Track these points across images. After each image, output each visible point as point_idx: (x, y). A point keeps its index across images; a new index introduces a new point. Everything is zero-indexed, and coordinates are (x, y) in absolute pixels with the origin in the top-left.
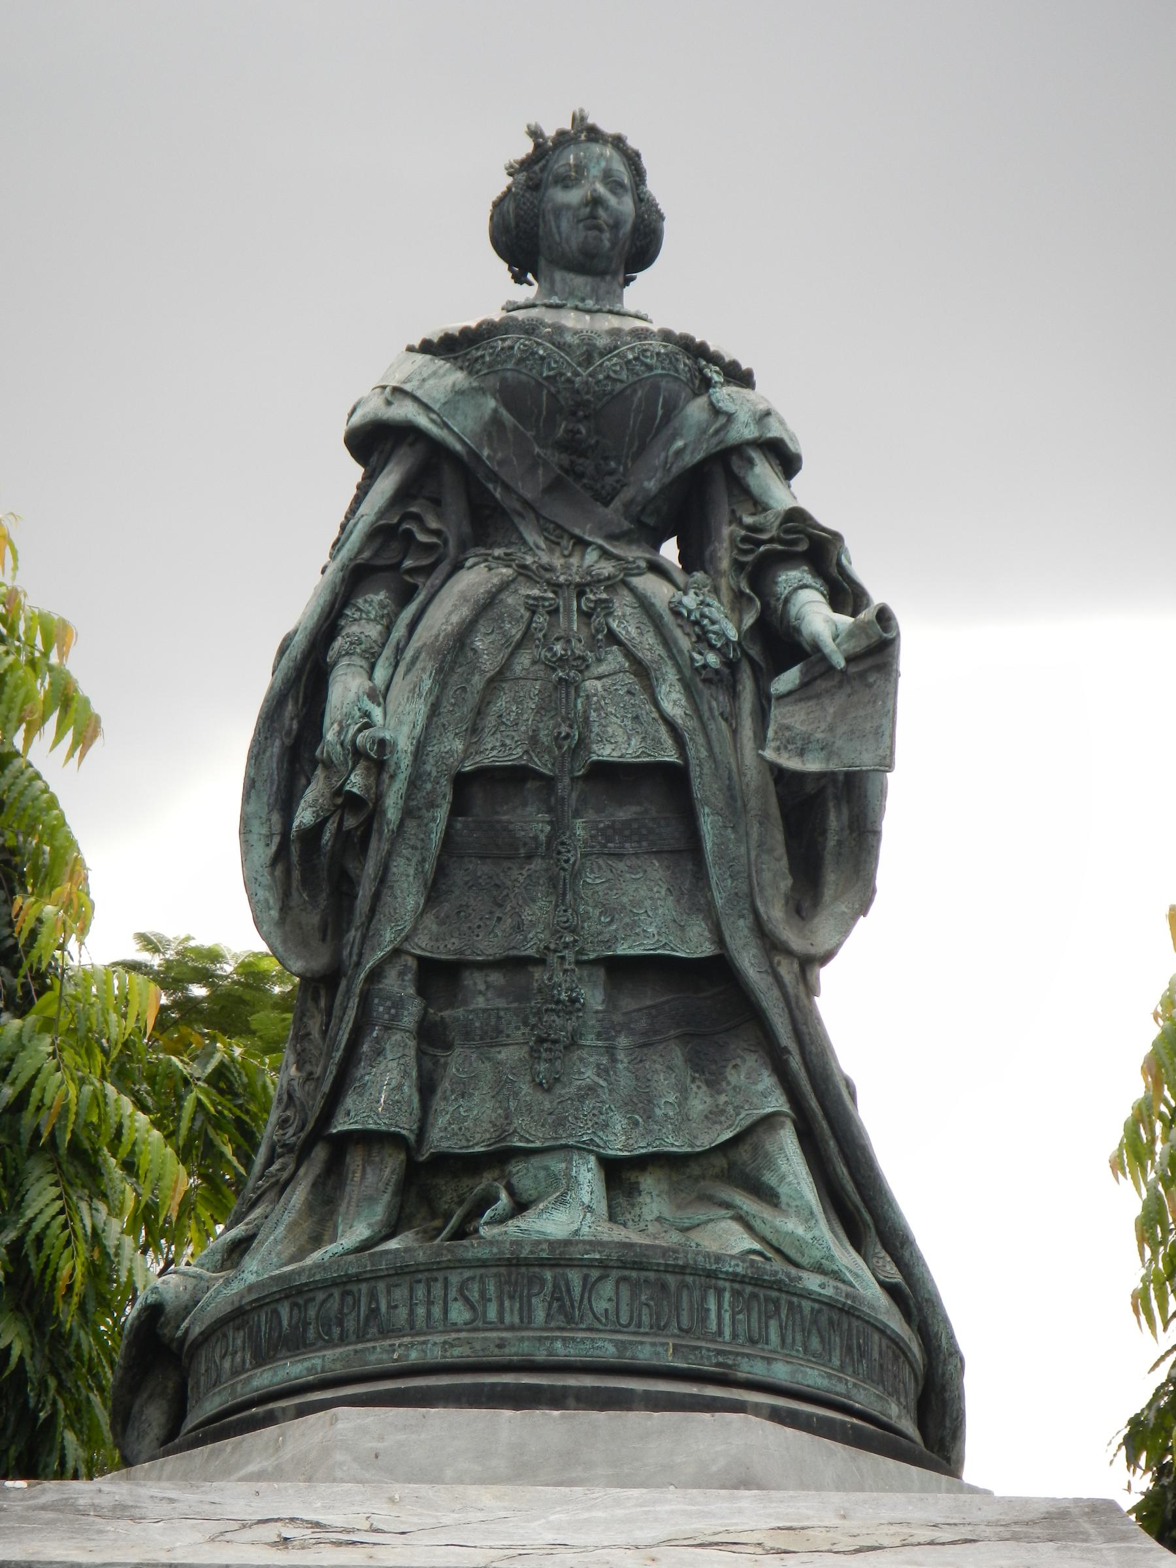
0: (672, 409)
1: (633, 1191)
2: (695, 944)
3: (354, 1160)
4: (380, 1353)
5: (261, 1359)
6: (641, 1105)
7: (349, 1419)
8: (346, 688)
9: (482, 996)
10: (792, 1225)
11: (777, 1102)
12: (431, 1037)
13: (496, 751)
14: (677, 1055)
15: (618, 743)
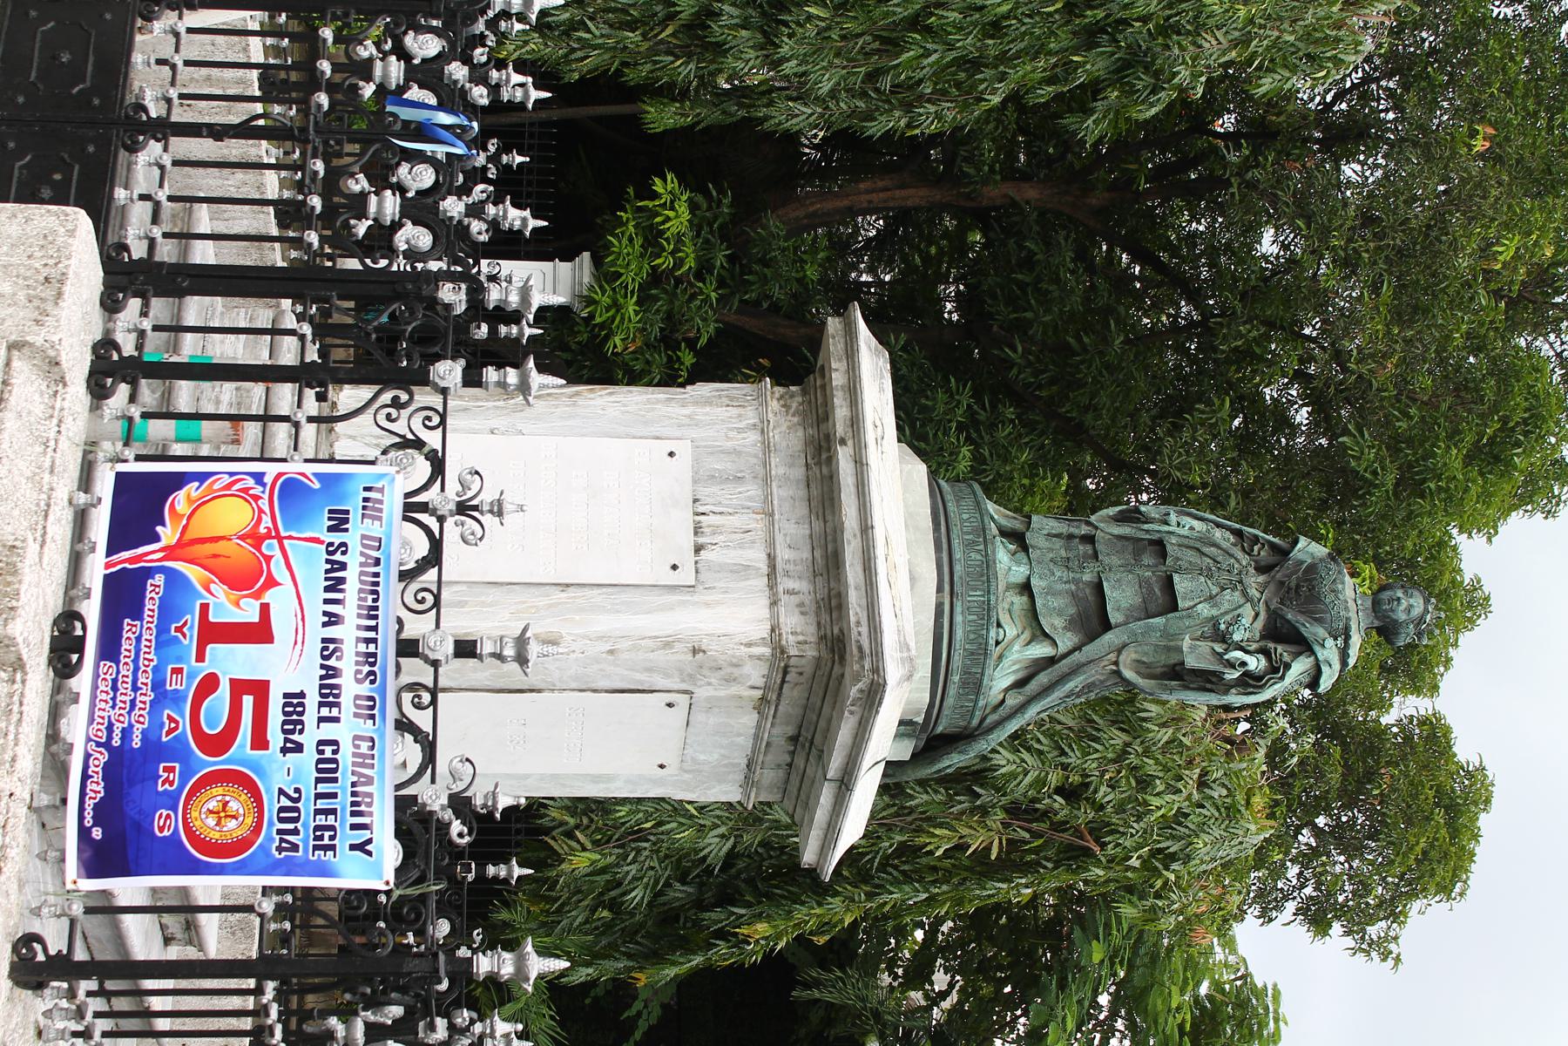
0: (1319, 621)
1: (1021, 594)
2: (1114, 617)
6: (1050, 591)
10: (1016, 647)
11: (1062, 648)
14: (1072, 611)
15: (1181, 584)
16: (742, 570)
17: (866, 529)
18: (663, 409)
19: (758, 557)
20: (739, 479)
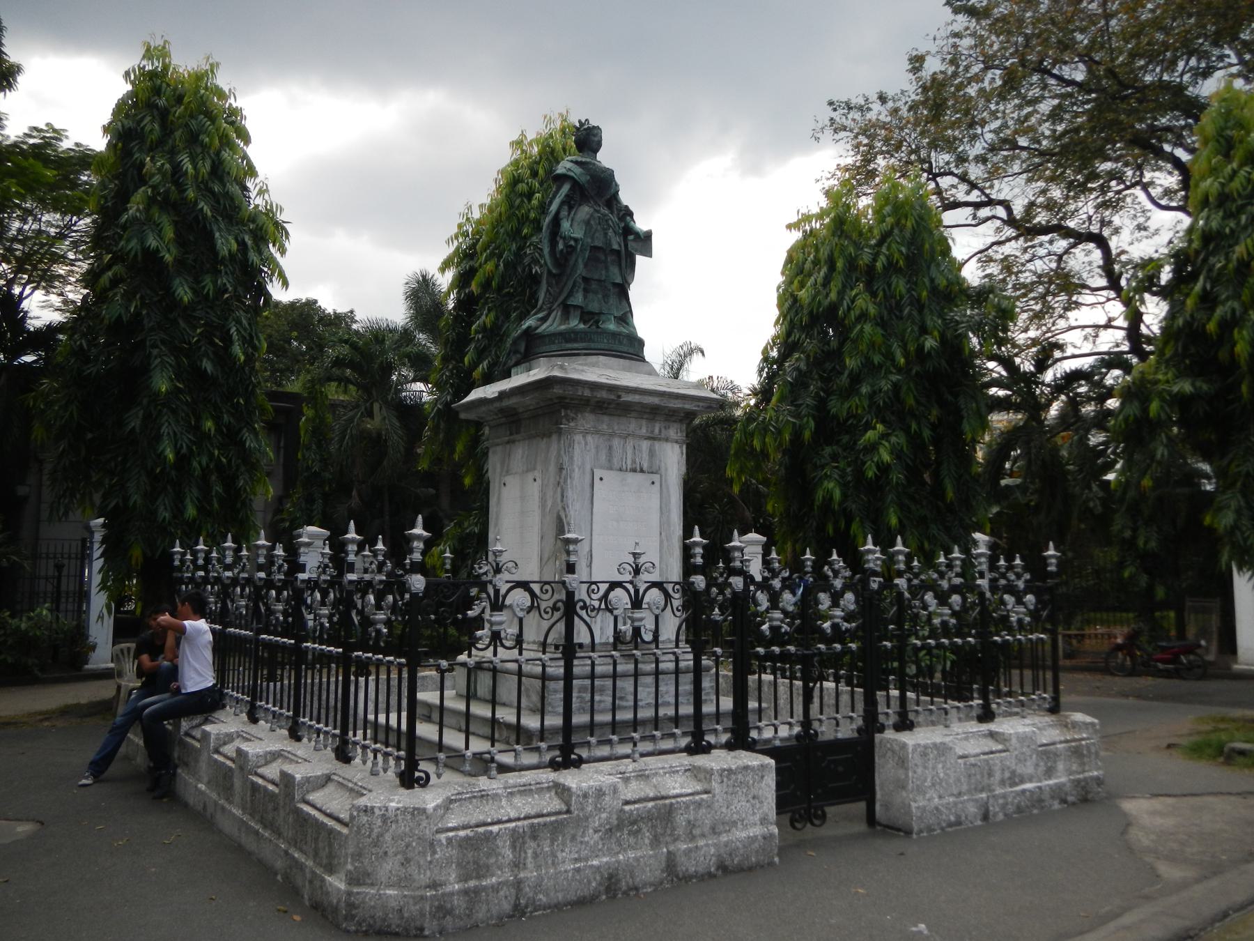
3: (572, 310)
4: (593, 345)
5: (567, 342)
7: (601, 358)
8: (565, 225)
9: (594, 286)
12: (586, 291)
13: (597, 243)
16: (652, 453)
17: (662, 394)
18: (576, 481)
19: (645, 445)
20: (610, 448)
